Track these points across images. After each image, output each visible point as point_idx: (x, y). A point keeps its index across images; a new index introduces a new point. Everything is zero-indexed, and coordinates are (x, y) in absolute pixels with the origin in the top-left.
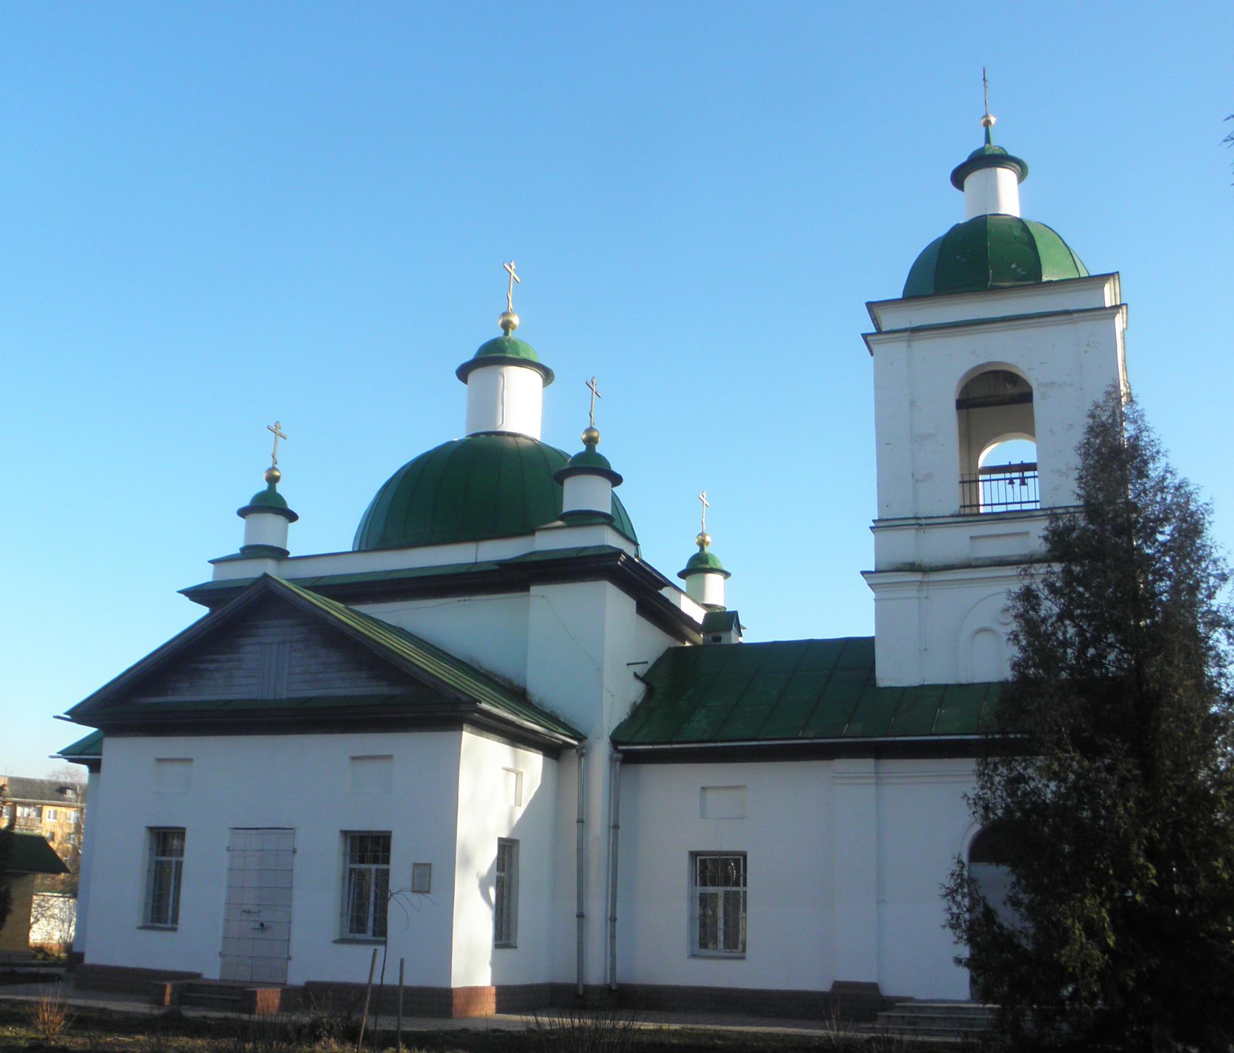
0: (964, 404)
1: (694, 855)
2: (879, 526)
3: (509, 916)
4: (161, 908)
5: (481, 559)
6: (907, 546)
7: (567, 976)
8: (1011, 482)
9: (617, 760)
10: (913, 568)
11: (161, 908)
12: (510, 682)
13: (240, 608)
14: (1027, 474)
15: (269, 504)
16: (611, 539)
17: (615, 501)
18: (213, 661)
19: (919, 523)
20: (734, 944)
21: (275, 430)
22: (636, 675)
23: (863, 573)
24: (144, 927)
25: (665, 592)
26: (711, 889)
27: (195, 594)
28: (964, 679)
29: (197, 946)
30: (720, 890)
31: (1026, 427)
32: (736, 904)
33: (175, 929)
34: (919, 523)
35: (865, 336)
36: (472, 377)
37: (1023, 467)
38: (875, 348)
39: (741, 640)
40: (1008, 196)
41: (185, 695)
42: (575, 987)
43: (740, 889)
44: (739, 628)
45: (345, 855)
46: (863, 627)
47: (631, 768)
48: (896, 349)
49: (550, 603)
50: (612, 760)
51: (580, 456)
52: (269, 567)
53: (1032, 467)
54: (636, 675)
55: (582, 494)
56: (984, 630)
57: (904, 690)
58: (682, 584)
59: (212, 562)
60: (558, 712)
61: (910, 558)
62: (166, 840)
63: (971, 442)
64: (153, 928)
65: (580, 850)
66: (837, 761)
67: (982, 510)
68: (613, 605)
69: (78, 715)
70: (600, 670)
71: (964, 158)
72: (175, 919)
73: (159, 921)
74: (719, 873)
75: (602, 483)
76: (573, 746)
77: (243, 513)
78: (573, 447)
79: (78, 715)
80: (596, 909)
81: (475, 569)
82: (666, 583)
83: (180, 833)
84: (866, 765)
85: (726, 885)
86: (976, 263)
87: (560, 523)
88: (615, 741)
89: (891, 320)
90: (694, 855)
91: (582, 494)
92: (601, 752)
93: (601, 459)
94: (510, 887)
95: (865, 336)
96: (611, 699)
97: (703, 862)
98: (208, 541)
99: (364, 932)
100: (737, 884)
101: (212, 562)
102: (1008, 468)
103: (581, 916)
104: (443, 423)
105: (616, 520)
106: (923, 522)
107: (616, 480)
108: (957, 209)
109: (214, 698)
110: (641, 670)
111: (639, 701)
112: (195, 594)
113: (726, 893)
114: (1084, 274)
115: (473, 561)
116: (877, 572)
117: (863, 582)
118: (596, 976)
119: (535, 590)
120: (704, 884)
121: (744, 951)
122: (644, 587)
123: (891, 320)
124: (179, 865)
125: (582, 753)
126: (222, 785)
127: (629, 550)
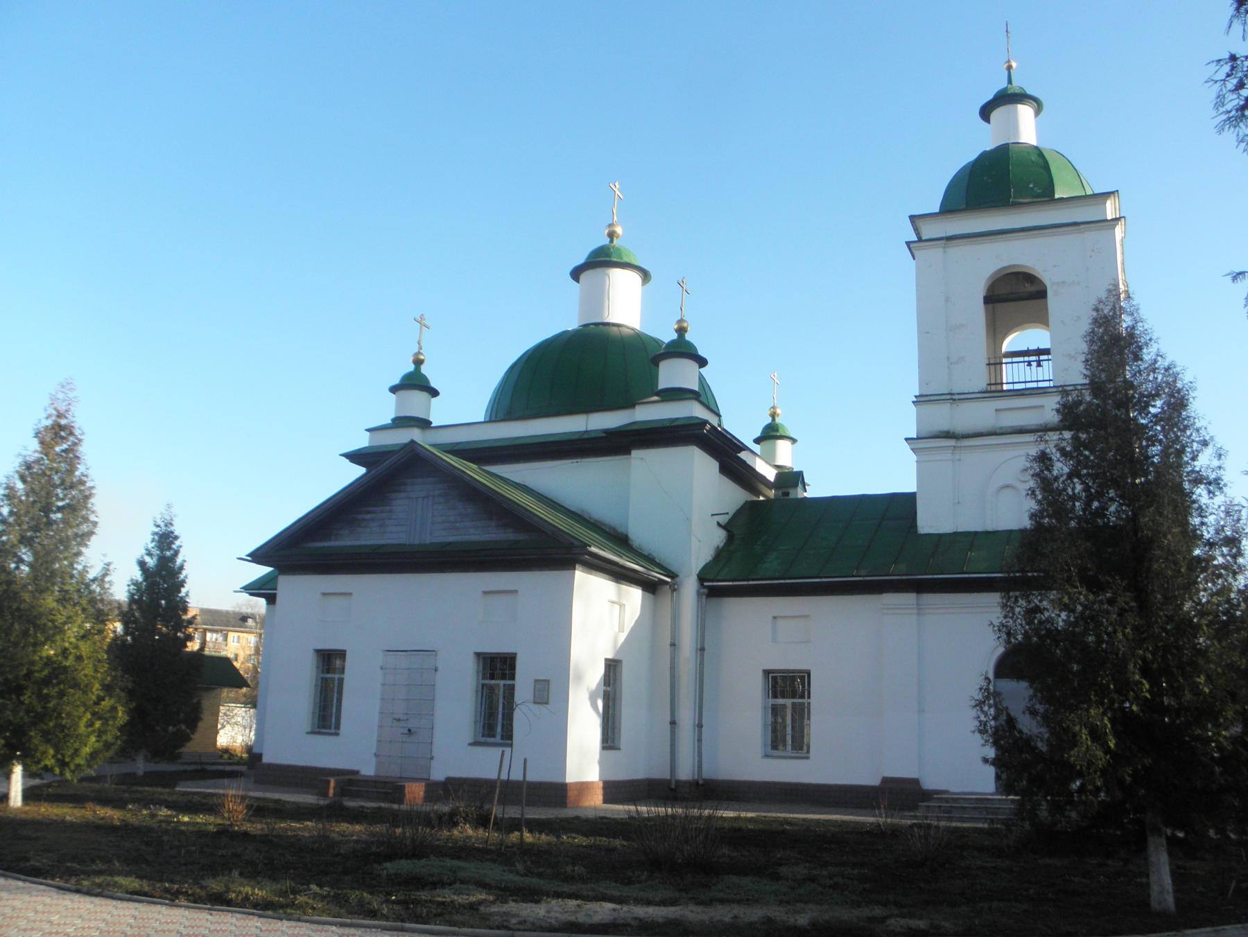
0: (990, 299)
1: (767, 673)
2: (921, 400)
3: (614, 723)
4: (326, 716)
6: (943, 417)
7: (662, 773)
8: (1029, 364)
10: (948, 435)
11: (326, 716)
12: (615, 530)
13: (391, 470)
14: (1042, 357)
15: (415, 382)
16: (698, 411)
17: (702, 380)
18: (369, 512)
19: (953, 398)
20: (800, 746)
21: (421, 321)
22: (719, 524)
23: (906, 439)
24: (312, 733)
25: (743, 455)
26: (780, 701)
27: (355, 457)
28: (990, 527)
29: (355, 749)
30: (788, 702)
31: (1042, 319)
32: (801, 713)
33: (337, 734)
34: (953, 398)
35: (908, 243)
36: (583, 277)
37: (1039, 352)
38: (916, 253)
39: (806, 494)
40: (1027, 127)
41: (346, 540)
42: (669, 782)
43: (805, 701)
44: (804, 485)
46: (907, 484)
47: (715, 600)
48: (933, 254)
50: (699, 594)
51: (672, 343)
52: (415, 434)
53: (1046, 352)
54: (719, 524)
55: (673, 374)
56: (1007, 486)
57: (940, 536)
58: (756, 448)
59: (368, 430)
60: (655, 555)
61: (946, 428)
62: (330, 660)
63: (996, 331)
64: (319, 733)
65: (673, 668)
66: (884, 595)
67: (1005, 387)
68: (699, 466)
69: (258, 556)
70: (689, 520)
71: (990, 97)
72: (338, 726)
73: (324, 727)
74: (787, 687)
75: (691, 365)
76: (666, 583)
77: (394, 390)
78: (667, 335)
79: (258, 556)
80: (686, 717)
81: (586, 436)
82: (743, 448)
83: (342, 654)
84: (909, 598)
86: (999, 182)
87: (656, 398)
88: (702, 578)
89: (929, 231)
90: (767, 673)
91: (673, 374)
92: (690, 587)
93: (690, 345)
94: (614, 700)
95: (908, 243)
96: (697, 544)
97: (774, 679)
98: (366, 413)
99: (494, 736)
100: (802, 696)
101: (368, 430)
102: (1027, 353)
103: (673, 723)
104: (559, 315)
105: (701, 395)
106: (956, 397)
107: (702, 362)
108: (984, 139)
110: (724, 520)
112: (355, 457)
113: (793, 704)
114: (1089, 192)
116: (918, 438)
117: (906, 447)
118: (685, 773)
119: (636, 453)
120: (775, 696)
121: (808, 752)
122: (725, 451)
123: (929, 231)
124: (341, 681)
125: (674, 589)
126: (376, 614)
127: (713, 420)
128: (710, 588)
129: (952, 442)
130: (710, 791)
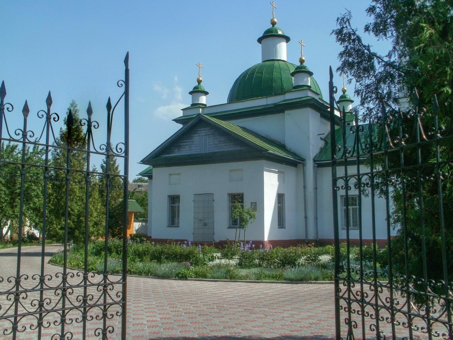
3: (283, 218)
5: (269, 103)
9: (315, 166)
12: (280, 143)
16: (310, 94)
22: (321, 138)
41: (177, 153)
45: (229, 201)
49: (292, 117)
50: (314, 167)
54: (321, 138)
60: (296, 152)
62: (174, 200)
65: (305, 196)
70: (308, 137)
80: (311, 215)
81: (267, 107)
85: (353, 206)
99: (237, 225)
103: (306, 217)
109: (186, 154)
110: (323, 136)
111: (323, 146)
113: (353, 208)
115: (266, 104)
118: (311, 236)
124: (179, 207)
125: (304, 165)
126: (189, 182)
127: (317, 98)
128: (318, 164)
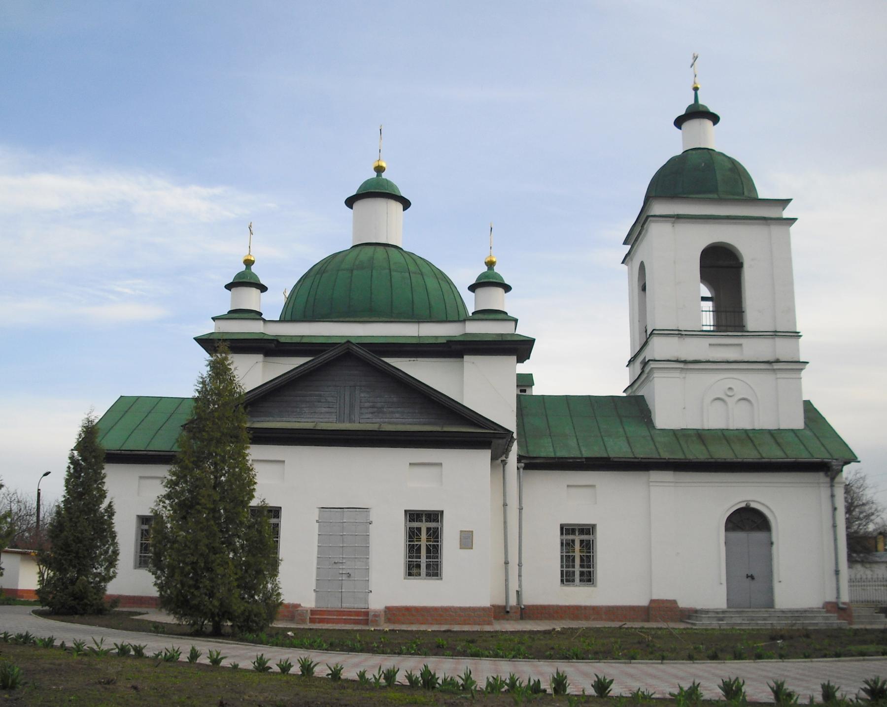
7: (501, 602)
42: (505, 607)
66: (651, 472)
129: (681, 365)
130: (526, 612)
